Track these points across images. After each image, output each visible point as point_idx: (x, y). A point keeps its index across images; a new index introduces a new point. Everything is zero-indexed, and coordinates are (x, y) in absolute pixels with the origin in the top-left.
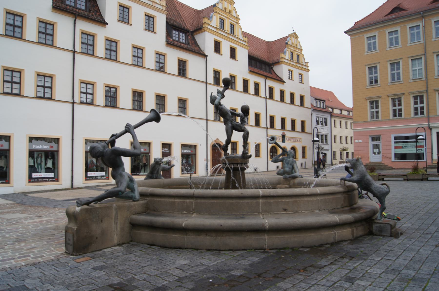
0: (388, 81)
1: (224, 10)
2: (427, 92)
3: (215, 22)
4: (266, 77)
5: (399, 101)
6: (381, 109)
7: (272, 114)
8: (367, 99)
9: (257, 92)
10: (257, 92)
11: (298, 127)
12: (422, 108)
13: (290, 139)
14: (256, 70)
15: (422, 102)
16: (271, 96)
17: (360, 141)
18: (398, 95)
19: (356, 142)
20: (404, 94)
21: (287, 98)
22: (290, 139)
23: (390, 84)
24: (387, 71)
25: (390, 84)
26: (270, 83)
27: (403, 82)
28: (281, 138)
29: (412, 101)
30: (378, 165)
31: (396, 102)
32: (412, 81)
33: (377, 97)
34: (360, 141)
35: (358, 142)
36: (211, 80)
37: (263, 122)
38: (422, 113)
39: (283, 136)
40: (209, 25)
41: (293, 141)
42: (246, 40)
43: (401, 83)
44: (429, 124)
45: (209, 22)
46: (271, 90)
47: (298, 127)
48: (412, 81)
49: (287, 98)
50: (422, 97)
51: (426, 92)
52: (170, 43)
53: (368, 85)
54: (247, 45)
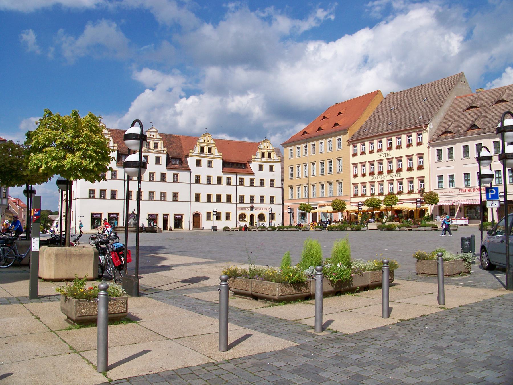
1: (204, 142)
3: (198, 149)
4: (236, 174)
7: (242, 194)
9: (229, 183)
10: (229, 183)
11: (267, 200)
13: (258, 209)
14: (229, 169)
16: (242, 184)
21: (257, 183)
22: (258, 209)
26: (239, 176)
28: (250, 208)
36: (193, 181)
37: (233, 200)
39: (252, 208)
40: (193, 153)
41: (261, 209)
42: (221, 154)
45: (193, 151)
46: (242, 180)
47: (267, 200)
49: (257, 183)
52: (169, 167)
54: (221, 157)
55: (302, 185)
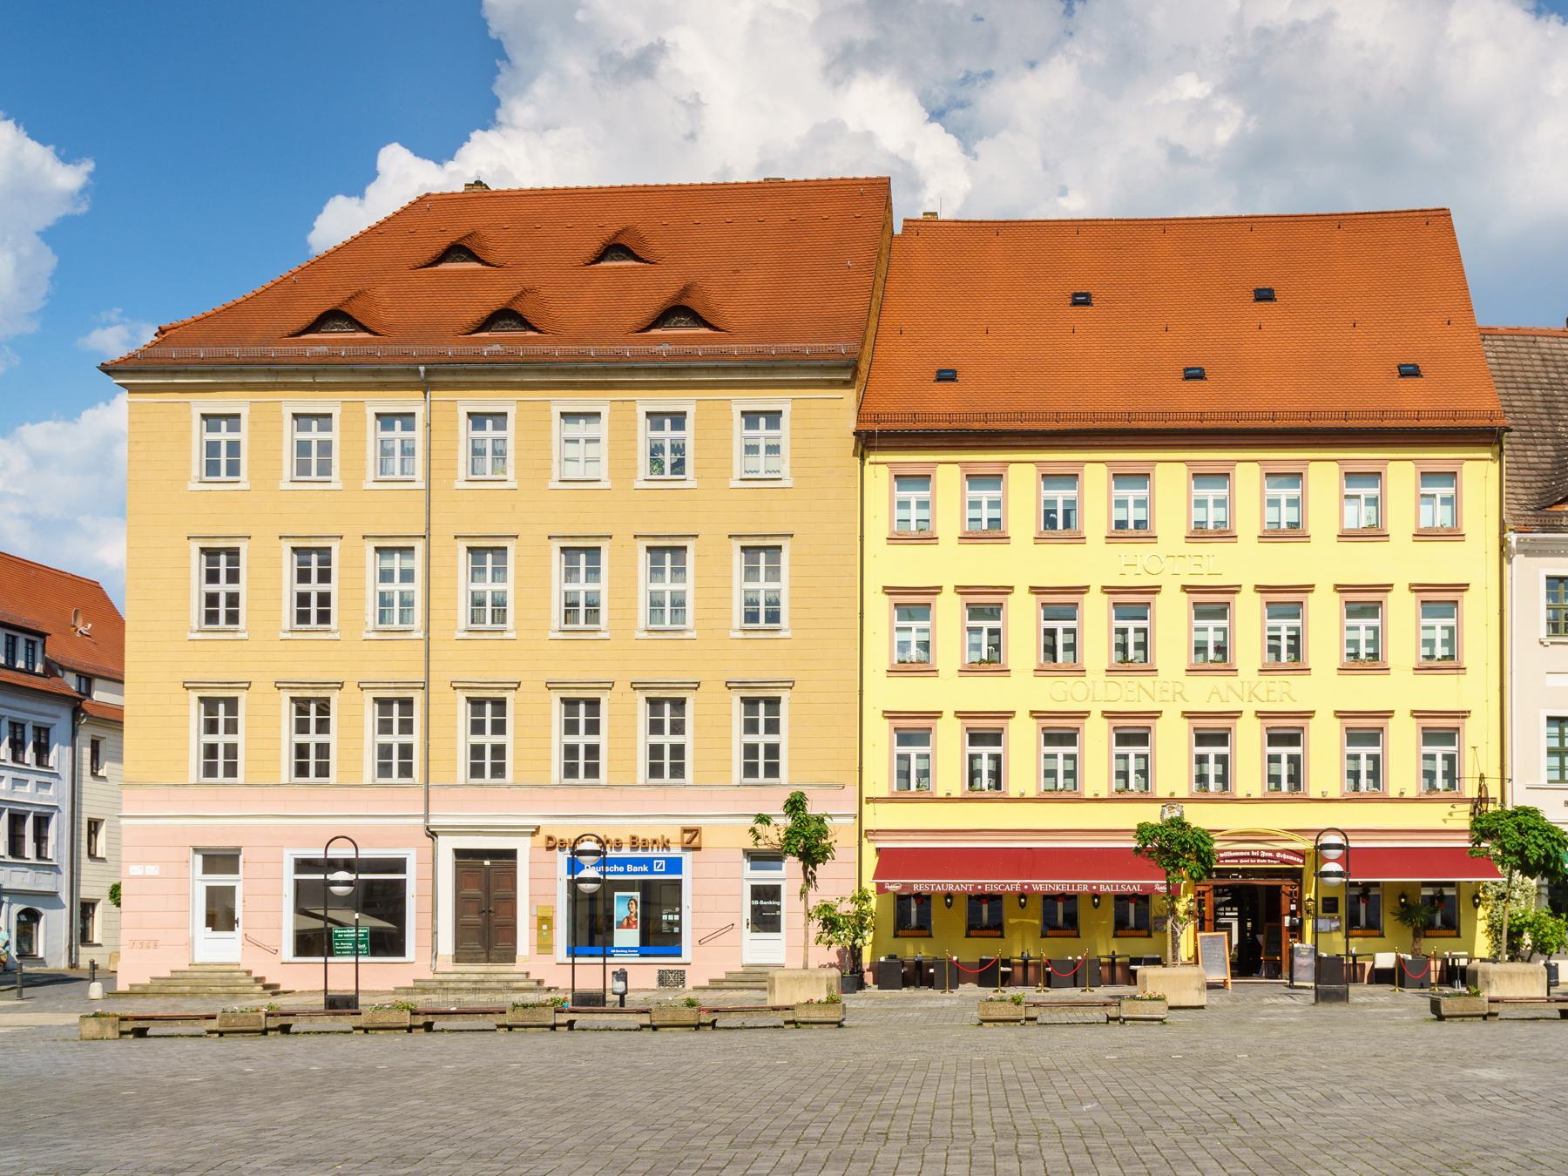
0: (279, 621)
2: (425, 687)
5: (319, 711)
6: (247, 739)
8: (187, 688)
12: (406, 751)
15: (406, 727)
17: (152, 870)
18: (315, 685)
19: (131, 873)
20: (340, 686)
23: (289, 635)
24: (280, 578)
25: (289, 635)
27: (337, 636)
29: (371, 714)
30: (222, 978)
31: (308, 713)
32: (373, 636)
33: (230, 685)
34: (152, 870)
35: (141, 873)
38: (406, 771)
43: (330, 636)
44: (427, 817)
48: (373, 636)
50: (407, 704)
51: (423, 688)
53: (196, 627)
55: (350, 687)
